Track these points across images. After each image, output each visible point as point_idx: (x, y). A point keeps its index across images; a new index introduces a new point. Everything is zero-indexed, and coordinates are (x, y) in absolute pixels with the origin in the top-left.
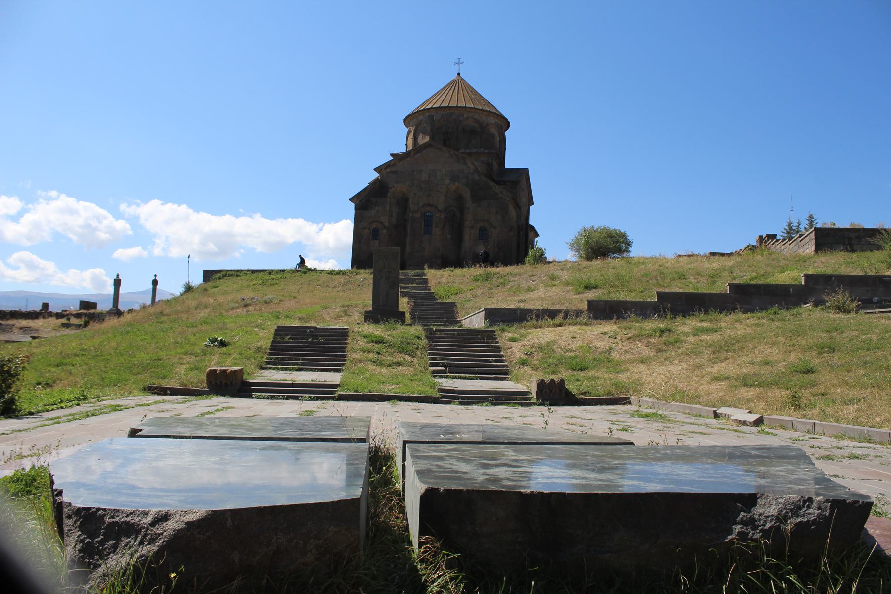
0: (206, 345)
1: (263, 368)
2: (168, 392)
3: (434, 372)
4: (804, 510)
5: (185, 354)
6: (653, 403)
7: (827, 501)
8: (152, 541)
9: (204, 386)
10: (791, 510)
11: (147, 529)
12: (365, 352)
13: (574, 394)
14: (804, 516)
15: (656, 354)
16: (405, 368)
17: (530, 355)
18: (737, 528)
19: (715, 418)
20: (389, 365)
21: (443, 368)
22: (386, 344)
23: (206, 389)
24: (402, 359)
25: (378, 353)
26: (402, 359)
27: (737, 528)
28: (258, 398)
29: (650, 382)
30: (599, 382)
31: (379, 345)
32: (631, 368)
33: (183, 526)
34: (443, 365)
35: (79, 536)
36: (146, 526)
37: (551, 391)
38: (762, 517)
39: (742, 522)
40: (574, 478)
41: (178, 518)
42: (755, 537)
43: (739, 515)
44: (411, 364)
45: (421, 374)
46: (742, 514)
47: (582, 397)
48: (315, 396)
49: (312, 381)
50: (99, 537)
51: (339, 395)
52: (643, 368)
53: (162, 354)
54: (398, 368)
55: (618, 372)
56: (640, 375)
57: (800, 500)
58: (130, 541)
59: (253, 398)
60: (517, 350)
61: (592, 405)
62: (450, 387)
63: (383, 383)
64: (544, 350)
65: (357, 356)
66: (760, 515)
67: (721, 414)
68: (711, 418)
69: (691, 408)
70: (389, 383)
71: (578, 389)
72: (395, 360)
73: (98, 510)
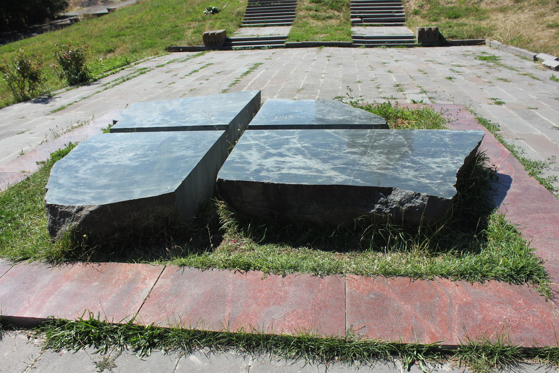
0: (205, 13)
1: (241, 27)
2: (181, 50)
3: (354, 22)
4: (414, 200)
5: (192, 21)
6: (499, 45)
7: (427, 196)
9: (202, 45)
10: (408, 199)
11: (75, 214)
12: (307, 10)
13: (445, 38)
15: (513, 4)
16: (334, 20)
17: (421, 7)
18: (377, 206)
20: (324, 19)
21: (360, 19)
22: (322, 4)
23: (204, 46)
24: (332, 14)
25: (316, 11)
26: (332, 14)
27: (377, 206)
28: (236, 49)
29: (502, 28)
30: (465, 28)
31: (317, 5)
33: (88, 213)
34: (360, 17)
36: (74, 213)
37: (428, 36)
38: (392, 201)
39: (381, 203)
41: (86, 210)
42: (386, 212)
43: (380, 199)
44: (338, 18)
45: (345, 24)
46: (382, 198)
47: (451, 40)
48: (271, 46)
49: (270, 35)
51: (287, 44)
52: (500, 16)
53: (178, 22)
54: (330, 20)
55: (481, 20)
56: (497, 21)
57: (413, 194)
58: (69, 220)
59: (232, 50)
60: (413, 3)
61: (457, 45)
62: (361, 34)
63: (317, 33)
64: (432, 2)
65: (302, 13)
66: (391, 200)
68: (532, 61)
70: (320, 33)
71: (449, 34)
72: (328, 15)
73: (56, 205)
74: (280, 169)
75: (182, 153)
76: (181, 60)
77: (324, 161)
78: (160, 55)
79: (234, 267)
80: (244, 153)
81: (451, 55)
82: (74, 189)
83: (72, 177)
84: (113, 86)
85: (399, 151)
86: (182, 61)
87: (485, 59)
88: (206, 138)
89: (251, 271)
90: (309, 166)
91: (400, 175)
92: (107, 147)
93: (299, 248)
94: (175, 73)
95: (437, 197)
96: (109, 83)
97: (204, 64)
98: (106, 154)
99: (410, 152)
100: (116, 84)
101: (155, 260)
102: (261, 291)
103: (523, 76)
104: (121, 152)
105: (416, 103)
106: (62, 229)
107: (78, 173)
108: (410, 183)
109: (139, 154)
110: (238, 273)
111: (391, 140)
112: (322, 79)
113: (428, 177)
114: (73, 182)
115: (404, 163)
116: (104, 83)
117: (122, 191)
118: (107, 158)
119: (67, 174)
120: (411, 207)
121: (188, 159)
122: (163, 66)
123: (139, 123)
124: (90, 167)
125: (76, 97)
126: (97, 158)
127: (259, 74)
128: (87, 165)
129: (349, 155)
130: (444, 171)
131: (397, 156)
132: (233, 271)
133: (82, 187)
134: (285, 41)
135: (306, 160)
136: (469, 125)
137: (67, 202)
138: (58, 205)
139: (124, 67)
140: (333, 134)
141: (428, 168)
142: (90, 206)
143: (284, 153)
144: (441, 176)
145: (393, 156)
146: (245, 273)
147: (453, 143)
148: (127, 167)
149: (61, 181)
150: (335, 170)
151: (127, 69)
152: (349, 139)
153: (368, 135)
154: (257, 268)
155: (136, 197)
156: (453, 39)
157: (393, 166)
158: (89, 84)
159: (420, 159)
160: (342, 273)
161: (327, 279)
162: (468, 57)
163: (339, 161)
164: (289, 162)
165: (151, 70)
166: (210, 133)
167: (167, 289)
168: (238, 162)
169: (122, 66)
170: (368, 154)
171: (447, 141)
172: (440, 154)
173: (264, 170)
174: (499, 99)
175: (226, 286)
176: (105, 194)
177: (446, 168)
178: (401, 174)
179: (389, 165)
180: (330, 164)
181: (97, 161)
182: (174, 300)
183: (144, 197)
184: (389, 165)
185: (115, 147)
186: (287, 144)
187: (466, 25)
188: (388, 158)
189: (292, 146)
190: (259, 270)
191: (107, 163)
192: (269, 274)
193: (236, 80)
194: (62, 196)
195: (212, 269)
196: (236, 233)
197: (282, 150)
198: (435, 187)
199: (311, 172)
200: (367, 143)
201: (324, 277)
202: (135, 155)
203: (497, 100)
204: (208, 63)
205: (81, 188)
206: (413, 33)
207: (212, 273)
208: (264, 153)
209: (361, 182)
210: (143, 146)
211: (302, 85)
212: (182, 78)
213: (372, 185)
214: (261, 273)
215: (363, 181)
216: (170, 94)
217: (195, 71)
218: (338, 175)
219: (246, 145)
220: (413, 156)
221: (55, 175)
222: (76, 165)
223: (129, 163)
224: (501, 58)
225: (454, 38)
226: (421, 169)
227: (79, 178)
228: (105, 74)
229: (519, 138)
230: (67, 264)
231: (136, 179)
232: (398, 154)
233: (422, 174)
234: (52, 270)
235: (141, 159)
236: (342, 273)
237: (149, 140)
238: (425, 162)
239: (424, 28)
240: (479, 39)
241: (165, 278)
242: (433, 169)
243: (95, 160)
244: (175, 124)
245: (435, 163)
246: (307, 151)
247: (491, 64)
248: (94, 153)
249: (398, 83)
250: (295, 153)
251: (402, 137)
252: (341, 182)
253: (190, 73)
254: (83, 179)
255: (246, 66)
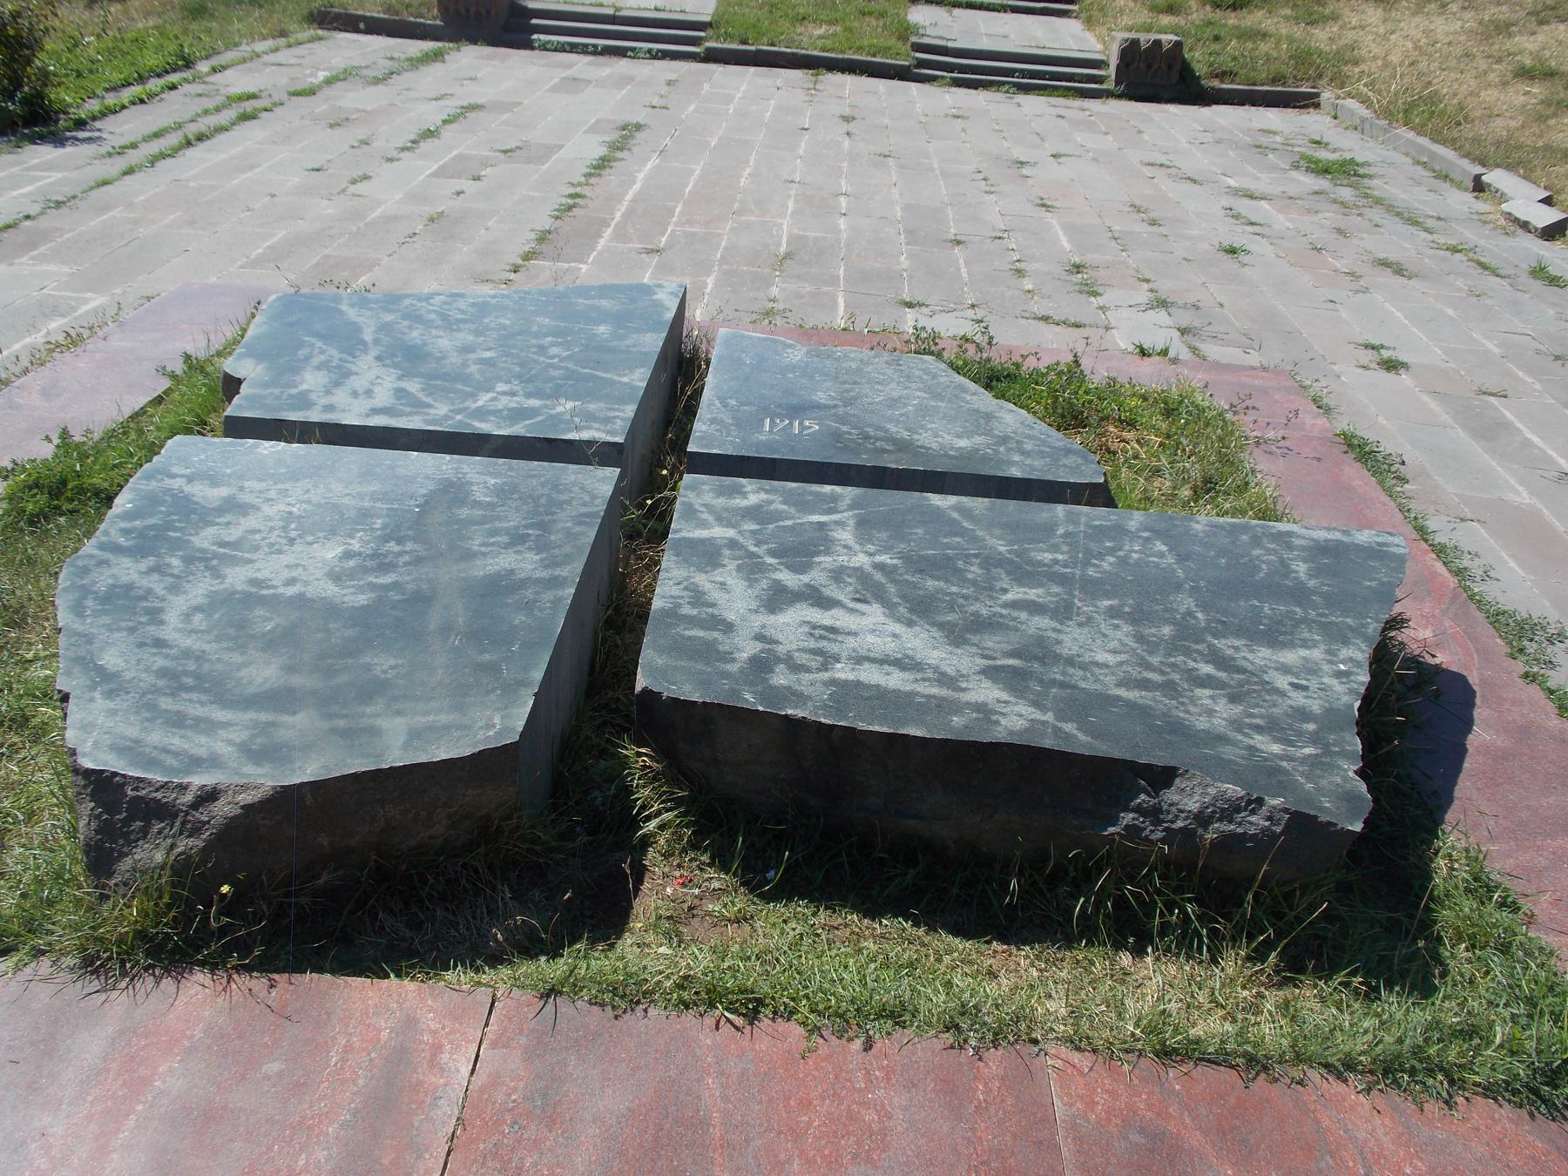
2: (362, 26)
4: (1243, 814)
6: (1363, 120)
7: (1286, 810)
8: (195, 831)
9: (433, 19)
10: (1223, 810)
11: (187, 813)
13: (1199, 77)
14: (1240, 824)
18: (1128, 818)
19: (1474, 190)
23: (438, 22)
27: (1128, 818)
28: (544, 47)
30: (1264, 47)
32: (1346, 12)
35: (92, 810)
36: (184, 808)
37: (1149, 66)
38: (1173, 809)
39: (1138, 810)
40: (904, 663)
42: (1153, 837)
43: (1137, 798)
46: (1143, 796)
47: (1216, 83)
48: (659, 51)
50: (120, 813)
51: (708, 49)
55: (1310, 23)
56: (1361, 33)
57: (1242, 798)
58: (164, 828)
59: (533, 48)
61: (1231, 104)
62: (940, 38)
63: (804, 18)
66: (1171, 805)
67: (1489, 185)
69: (1433, 155)
70: (814, 21)
71: (1211, 65)
73: (115, 774)
74: (828, 660)
75: (505, 561)
76: (371, 73)
77: (956, 636)
78: (292, 40)
79: (712, 1005)
80: (701, 580)
81: (1218, 142)
82: (166, 703)
83: (145, 644)
84: (154, 160)
85: (1166, 610)
86: (377, 81)
87: (1324, 170)
88: (564, 497)
89: (765, 1022)
90: (910, 653)
91: (1189, 713)
92: (233, 507)
93: (885, 922)
94: (361, 133)
95: (1316, 817)
96: (134, 146)
97: (451, 106)
98: (242, 538)
99: (1200, 615)
100: (163, 156)
101: (455, 967)
102: (806, 1104)
103: (1448, 254)
104: (293, 534)
105: (1149, 355)
106: (137, 857)
107: (162, 622)
108: (1228, 752)
109: (360, 554)
110: (726, 1028)
111: (1135, 556)
112: (842, 220)
113: (1272, 727)
114: (155, 668)
115: (1192, 664)
116: (118, 142)
117: (341, 723)
118: (250, 561)
119: (123, 624)
120: (1233, 835)
121: (529, 593)
122: (311, 92)
123: (324, 401)
124: (200, 600)
125: (24, 195)
126: (216, 556)
127: (641, 176)
128: (187, 586)
129: (1024, 616)
130: (1315, 706)
131: (1167, 630)
132: (709, 1021)
133: (195, 696)
134: (701, 38)
135: (898, 628)
136: (1319, 460)
137: (152, 763)
138: (124, 776)
139: (174, 78)
140: (955, 515)
141: (1269, 692)
142: (244, 788)
143: (823, 590)
144: (1311, 727)
145: (1153, 631)
146: (749, 1027)
147: (1323, 584)
148: (331, 610)
149: (111, 659)
150: (995, 681)
151: (187, 88)
152: (1010, 543)
153: (1061, 531)
154: (782, 1008)
155: (396, 756)
156: (1222, 82)
157: (1163, 673)
158: (58, 140)
159: (1236, 649)
160: (1035, 1042)
161: (994, 1057)
162: (1270, 156)
163: (998, 638)
164: (849, 634)
165: (275, 105)
166: (573, 478)
167: (515, 1090)
168: (692, 621)
169: (167, 72)
170: (1078, 615)
171: (1303, 576)
172: (1292, 634)
173: (779, 660)
174: (1388, 348)
175: (698, 1081)
176: (284, 735)
177: (1322, 694)
178: (1191, 708)
179: (1148, 667)
180: (974, 650)
181: (217, 575)
182: (547, 1139)
183: (423, 758)
184: (1148, 667)
185: (267, 510)
186: (827, 552)
187: (1265, 36)
188: (1140, 638)
189: (843, 559)
190: (789, 1020)
191: (254, 582)
192: (822, 1036)
193: (572, 191)
194: (132, 732)
195: (646, 1010)
196: (684, 851)
197: (815, 577)
198: (1302, 774)
199: (924, 680)
200: (1065, 566)
201: (986, 1055)
202: (348, 555)
203: (1386, 354)
204: (465, 104)
205: (191, 701)
206: (1099, 47)
207: (647, 1026)
208: (764, 584)
209: (1081, 736)
210: (365, 515)
211: (784, 241)
212: (391, 160)
213: (1117, 754)
214: (795, 1030)
215: (1086, 733)
216: (361, 225)
217: (429, 134)
218: (1005, 702)
219: (702, 541)
220: (1215, 636)
221: (77, 626)
222: (144, 582)
223: (331, 590)
224: (1371, 170)
225: (1227, 79)
226: (1248, 693)
227: (171, 647)
228: (111, 100)
229: (1469, 516)
230: (158, 980)
231: (377, 671)
232: (1166, 622)
233: (1252, 716)
234: (107, 1005)
235: (372, 579)
236: (1035, 1042)
237: (375, 487)
238: (1252, 663)
239: (1138, 40)
240: (1302, 89)
241: (504, 1046)
242: (1283, 694)
243: (209, 562)
244: (446, 418)
245: (1285, 669)
246: (892, 589)
247: (1346, 193)
248: (197, 534)
249: (1077, 260)
250: (857, 592)
251: (1164, 548)
252: (1020, 733)
253: (414, 142)
254: (187, 654)
255: (593, 130)
